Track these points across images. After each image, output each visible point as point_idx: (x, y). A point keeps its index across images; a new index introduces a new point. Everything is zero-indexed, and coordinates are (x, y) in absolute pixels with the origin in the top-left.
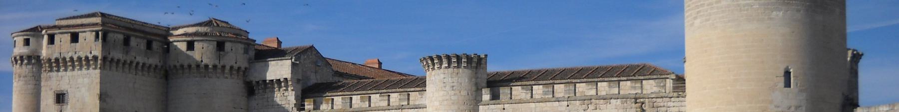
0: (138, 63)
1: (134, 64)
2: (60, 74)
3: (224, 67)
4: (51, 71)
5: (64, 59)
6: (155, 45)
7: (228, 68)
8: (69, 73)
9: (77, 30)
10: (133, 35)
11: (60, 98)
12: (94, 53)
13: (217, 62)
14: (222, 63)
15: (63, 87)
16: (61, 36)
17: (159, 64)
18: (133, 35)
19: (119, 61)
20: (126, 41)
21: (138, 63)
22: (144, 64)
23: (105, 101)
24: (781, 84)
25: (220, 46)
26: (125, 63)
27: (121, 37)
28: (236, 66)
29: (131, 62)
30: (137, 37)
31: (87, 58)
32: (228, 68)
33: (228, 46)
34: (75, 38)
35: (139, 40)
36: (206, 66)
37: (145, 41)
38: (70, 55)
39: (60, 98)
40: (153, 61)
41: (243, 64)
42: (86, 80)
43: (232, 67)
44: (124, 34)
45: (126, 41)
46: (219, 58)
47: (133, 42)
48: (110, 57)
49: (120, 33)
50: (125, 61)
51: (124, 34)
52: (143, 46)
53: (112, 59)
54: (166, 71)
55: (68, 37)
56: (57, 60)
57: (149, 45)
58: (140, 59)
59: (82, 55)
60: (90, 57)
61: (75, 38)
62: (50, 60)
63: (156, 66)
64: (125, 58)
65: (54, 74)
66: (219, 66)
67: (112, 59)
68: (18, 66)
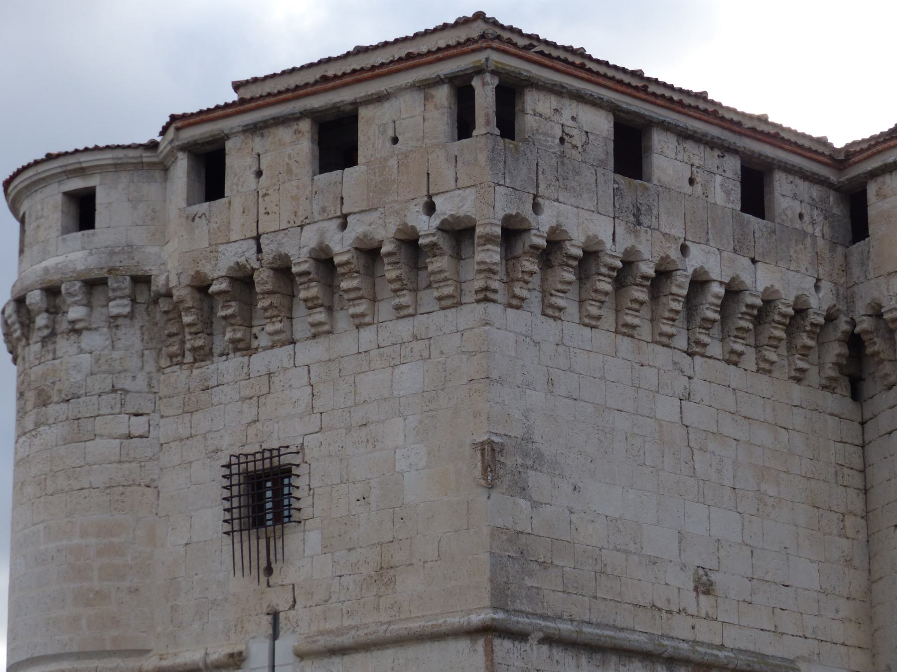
1: (680, 286)
2: (259, 362)
4: (203, 355)
5: (283, 270)
8: (311, 352)
9: (346, 96)
10: (666, 127)
11: (263, 496)
12: (445, 207)
15: (282, 428)
16: (258, 143)
18: (666, 127)
19: (591, 255)
20: (630, 151)
21: (699, 283)
22: (733, 291)
23: (523, 490)
27: (602, 124)
29: (664, 274)
30: (685, 135)
31: (410, 243)
34: (336, 142)
35: (697, 154)
37: (733, 164)
38: (310, 238)
39: (263, 496)
40: (786, 276)
42: (410, 377)
44: (614, 109)
47: (667, 159)
48: (545, 222)
50: (629, 263)
51: (614, 109)
52: (723, 188)
53: (556, 240)
54: (855, 342)
55: (298, 145)
56: (243, 280)
59: (383, 230)
60: (425, 226)
61: (336, 142)
62: (202, 287)
63: (801, 311)
65: (228, 367)
67: (556, 240)
68: (36, 348)
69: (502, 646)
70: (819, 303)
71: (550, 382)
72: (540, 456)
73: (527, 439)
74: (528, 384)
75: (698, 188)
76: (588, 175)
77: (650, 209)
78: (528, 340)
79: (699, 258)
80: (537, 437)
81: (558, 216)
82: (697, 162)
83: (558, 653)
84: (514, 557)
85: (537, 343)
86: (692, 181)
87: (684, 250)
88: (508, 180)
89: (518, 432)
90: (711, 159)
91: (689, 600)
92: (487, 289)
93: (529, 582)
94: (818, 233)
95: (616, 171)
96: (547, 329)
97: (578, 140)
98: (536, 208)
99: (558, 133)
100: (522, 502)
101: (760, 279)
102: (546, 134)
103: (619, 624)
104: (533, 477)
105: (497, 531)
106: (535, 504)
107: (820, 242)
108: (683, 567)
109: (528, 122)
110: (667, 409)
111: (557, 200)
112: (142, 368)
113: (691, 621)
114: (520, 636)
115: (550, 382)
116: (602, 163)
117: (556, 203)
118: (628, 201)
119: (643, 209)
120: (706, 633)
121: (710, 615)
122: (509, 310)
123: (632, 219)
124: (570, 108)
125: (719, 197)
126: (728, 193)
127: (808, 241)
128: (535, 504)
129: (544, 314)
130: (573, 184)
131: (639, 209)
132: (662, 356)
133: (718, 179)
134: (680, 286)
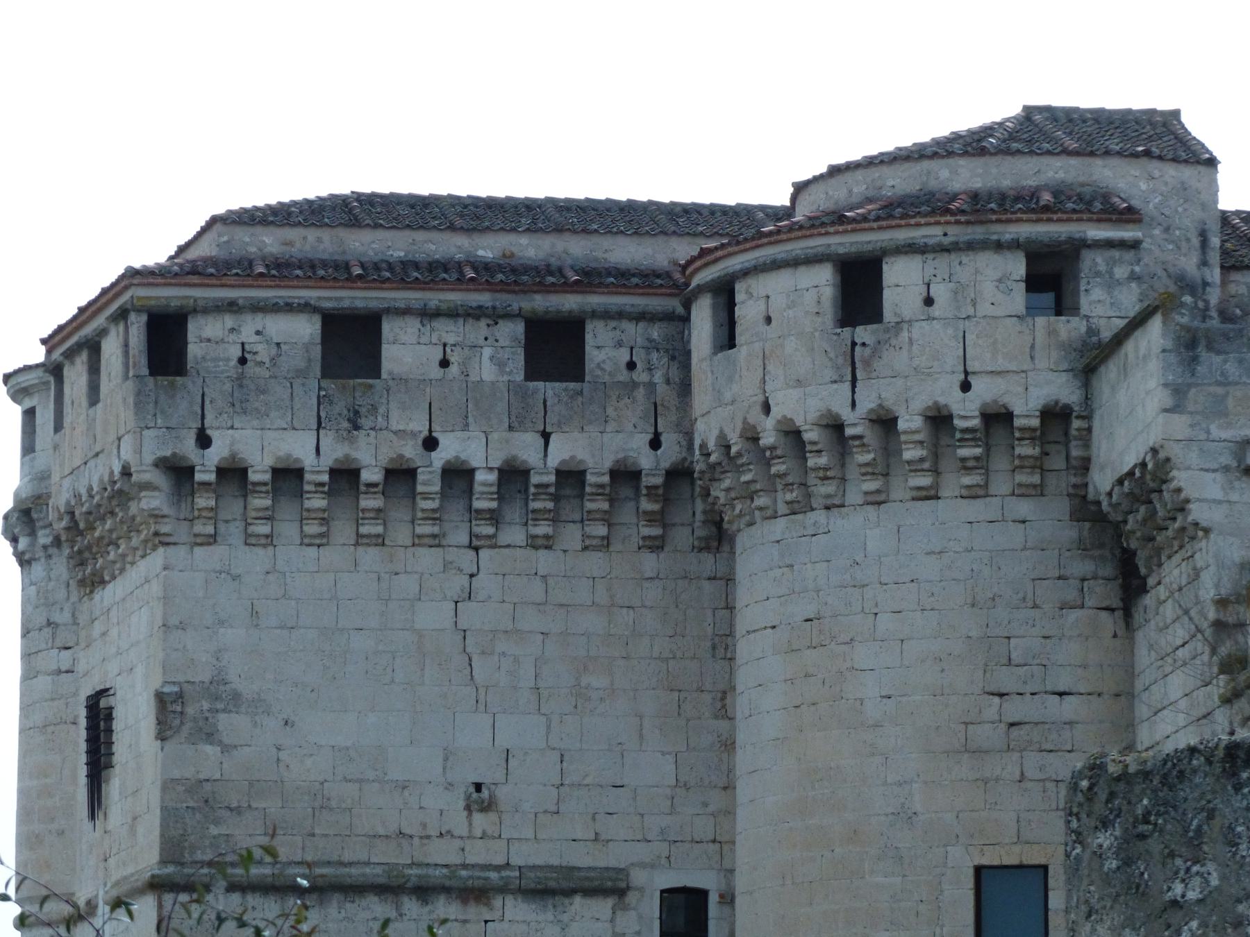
0: (458, 476)
1: (429, 481)
3: (885, 423)
6: (603, 349)
7: (910, 422)
13: (836, 400)
14: (867, 402)
17: (646, 461)
19: (287, 477)
20: (351, 345)
22: (513, 476)
23: (210, 736)
25: (859, 293)
26: (345, 477)
27: (306, 329)
28: (966, 411)
29: (400, 476)
32: (910, 422)
33: (902, 281)
35: (449, 331)
36: (793, 434)
41: (1033, 390)
43: (939, 420)
45: (351, 345)
46: (853, 371)
47: (405, 349)
48: (216, 454)
49: (289, 308)
52: (494, 356)
57: (554, 349)
58: (474, 447)
64: (334, 451)
71: (254, 613)
72: (236, 696)
73: (219, 680)
74: (221, 623)
75: (454, 369)
76: (280, 391)
77: (374, 409)
78: (223, 575)
79: (450, 448)
80: (232, 676)
81: (232, 444)
82: (451, 339)
84: (189, 805)
85: (235, 578)
86: (444, 363)
87: (430, 444)
88: (159, 421)
89: (205, 676)
90: (477, 331)
91: (458, 821)
92: (156, 534)
93: (214, 830)
94: (658, 377)
96: (254, 561)
97: (263, 352)
98: (204, 441)
99: (236, 352)
100: (209, 749)
101: (562, 450)
102: (216, 360)
103: (347, 858)
105: (168, 785)
106: (226, 748)
107: (662, 389)
109: (194, 350)
110: (434, 616)
111: (232, 428)
112: (68, 598)
113: (458, 843)
115: (254, 613)
116: (302, 373)
117: (230, 431)
118: (340, 406)
119: (363, 410)
120: (478, 854)
121: (489, 832)
122: (197, 550)
123: (346, 425)
124: (249, 326)
125: (487, 371)
126: (501, 365)
127: (640, 393)
128: (226, 748)
129: (246, 544)
130: (257, 404)
131: (357, 413)
132: (427, 558)
133: (487, 352)
134: (429, 481)
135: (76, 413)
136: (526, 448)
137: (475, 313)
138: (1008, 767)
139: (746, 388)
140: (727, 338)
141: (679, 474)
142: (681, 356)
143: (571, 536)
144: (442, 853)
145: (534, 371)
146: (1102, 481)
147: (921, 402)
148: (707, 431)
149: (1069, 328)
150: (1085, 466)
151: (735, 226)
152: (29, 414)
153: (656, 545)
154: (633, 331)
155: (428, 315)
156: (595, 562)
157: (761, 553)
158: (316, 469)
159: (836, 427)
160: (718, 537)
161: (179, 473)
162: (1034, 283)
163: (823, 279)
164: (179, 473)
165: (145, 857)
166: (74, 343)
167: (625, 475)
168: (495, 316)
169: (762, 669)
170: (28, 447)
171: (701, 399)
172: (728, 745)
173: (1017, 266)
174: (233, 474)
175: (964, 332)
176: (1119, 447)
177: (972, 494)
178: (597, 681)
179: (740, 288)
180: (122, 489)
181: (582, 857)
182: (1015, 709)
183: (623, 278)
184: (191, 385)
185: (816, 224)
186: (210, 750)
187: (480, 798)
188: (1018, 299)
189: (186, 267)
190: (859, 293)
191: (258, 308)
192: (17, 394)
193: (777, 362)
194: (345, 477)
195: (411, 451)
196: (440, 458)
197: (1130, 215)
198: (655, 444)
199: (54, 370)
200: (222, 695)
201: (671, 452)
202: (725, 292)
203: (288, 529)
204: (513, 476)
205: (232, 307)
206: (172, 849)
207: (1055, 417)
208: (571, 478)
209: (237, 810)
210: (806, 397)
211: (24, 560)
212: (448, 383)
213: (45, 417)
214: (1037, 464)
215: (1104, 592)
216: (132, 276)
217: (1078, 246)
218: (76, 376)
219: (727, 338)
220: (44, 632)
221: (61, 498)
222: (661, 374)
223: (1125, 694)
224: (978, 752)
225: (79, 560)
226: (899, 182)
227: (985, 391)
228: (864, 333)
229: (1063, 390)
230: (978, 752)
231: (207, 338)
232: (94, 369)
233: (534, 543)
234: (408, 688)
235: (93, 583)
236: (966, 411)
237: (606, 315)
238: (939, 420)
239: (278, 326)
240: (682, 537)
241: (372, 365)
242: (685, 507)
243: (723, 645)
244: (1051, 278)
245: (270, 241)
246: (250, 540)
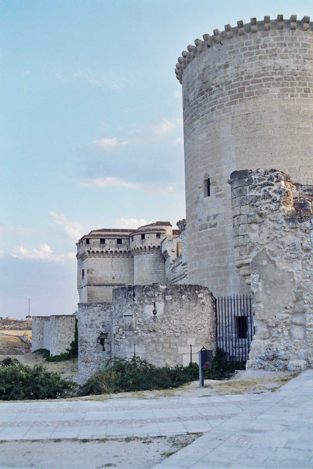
0: (111, 252)
3: (145, 247)
6: (123, 241)
14: (144, 246)
20: (103, 241)
22: (116, 252)
23: (92, 273)
24: (202, 195)
25: (143, 237)
26: (102, 252)
27: (99, 240)
28: (152, 247)
29: (107, 252)
32: (147, 247)
33: (146, 236)
35: (111, 240)
36: (138, 248)
40: (122, 249)
45: (103, 241)
47: (107, 241)
52: (114, 242)
57: (119, 241)
58: (113, 250)
64: (101, 250)
66: (143, 248)
69: (89, 287)
70: (127, 251)
72: (94, 270)
73: (92, 269)
76: (97, 245)
83: (95, 286)
87: (109, 249)
89: (91, 268)
91: (112, 280)
95: (101, 244)
98: (91, 249)
101: (120, 250)
104: (92, 272)
108: (111, 277)
109: (90, 242)
110: (110, 263)
114: (91, 285)
120: (113, 283)
124: (94, 240)
132: (109, 258)
135: (81, 247)
136: (117, 249)
137: (113, 239)
138: (155, 275)
139: (134, 245)
140: (133, 241)
141: (129, 251)
142: (129, 242)
143: (121, 257)
144: (110, 282)
145: (118, 243)
146: (162, 252)
147: (148, 246)
148: (131, 248)
149: (160, 240)
150: (161, 251)
151: (134, 231)
152: (78, 247)
153: (128, 257)
154: (126, 240)
155: (109, 239)
156: (123, 259)
157: (135, 257)
158: (100, 251)
159: (141, 248)
160: (133, 257)
161: (89, 252)
162: (157, 236)
163: (140, 236)
164: (89, 252)
165: (86, 283)
166: (81, 241)
167: (125, 252)
168: (114, 239)
169: (136, 268)
170: (78, 249)
171: (131, 245)
172: (133, 273)
173: (156, 235)
174: (93, 252)
175: (151, 240)
176: (163, 250)
177: (152, 253)
178: (123, 268)
179: (134, 237)
180: (84, 253)
181: (122, 283)
182: (156, 271)
183: (125, 236)
184: (90, 245)
185: (140, 231)
186: (91, 274)
187: (113, 278)
188: (156, 237)
189: (90, 235)
190: (143, 237)
191: (95, 238)
192: (77, 245)
193: (137, 243)
194: (102, 252)
195: (108, 250)
196: (110, 250)
197: (165, 230)
198: (128, 249)
199: (80, 243)
200: (92, 270)
201: (129, 250)
202: (132, 237)
203: (97, 256)
204: (116, 252)
205: (93, 238)
206: (89, 283)
207: (159, 247)
208: (121, 252)
209: (94, 279)
210: (139, 245)
211: (78, 259)
212: (111, 245)
213: (79, 247)
214: (158, 251)
215: (164, 261)
216: (85, 236)
217: (161, 233)
218: (81, 244)
219: (133, 241)
220: (79, 264)
221: (80, 254)
222: (127, 243)
223: (164, 269)
224: (152, 274)
225: (82, 258)
226: (146, 228)
227: (153, 245)
228: (143, 240)
229: (160, 245)
230: (152, 274)
231: (91, 241)
232: (82, 243)
233: (118, 257)
234: (107, 269)
235: (83, 260)
236: (152, 247)
237: (123, 239)
238: (149, 247)
239: (97, 240)
240: (130, 257)
241: (104, 243)
242: (130, 254)
243: (133, 265)
244: (158, 236)
245: (97, 233)
246: (95, 257)
